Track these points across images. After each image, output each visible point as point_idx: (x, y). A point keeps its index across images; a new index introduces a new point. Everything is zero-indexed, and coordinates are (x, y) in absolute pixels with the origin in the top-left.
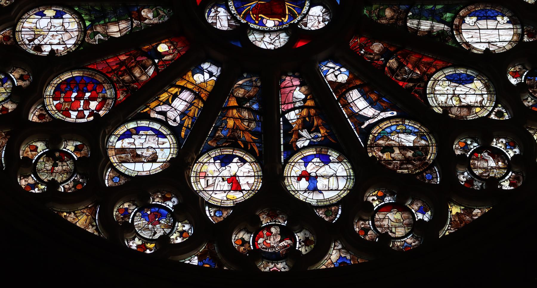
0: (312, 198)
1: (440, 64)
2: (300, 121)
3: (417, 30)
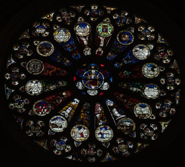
0: (102, 140)
1: (138, 101)
2: (100, 117)
3: (133, 91)
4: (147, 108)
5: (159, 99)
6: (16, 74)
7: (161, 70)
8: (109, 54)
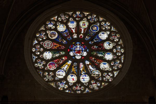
0: (84, 82)
1: (102, 61)
4: (107, 65)
5: (114, 60)
6: (38, 49)
7: (114, 45)
8: (87, 37)
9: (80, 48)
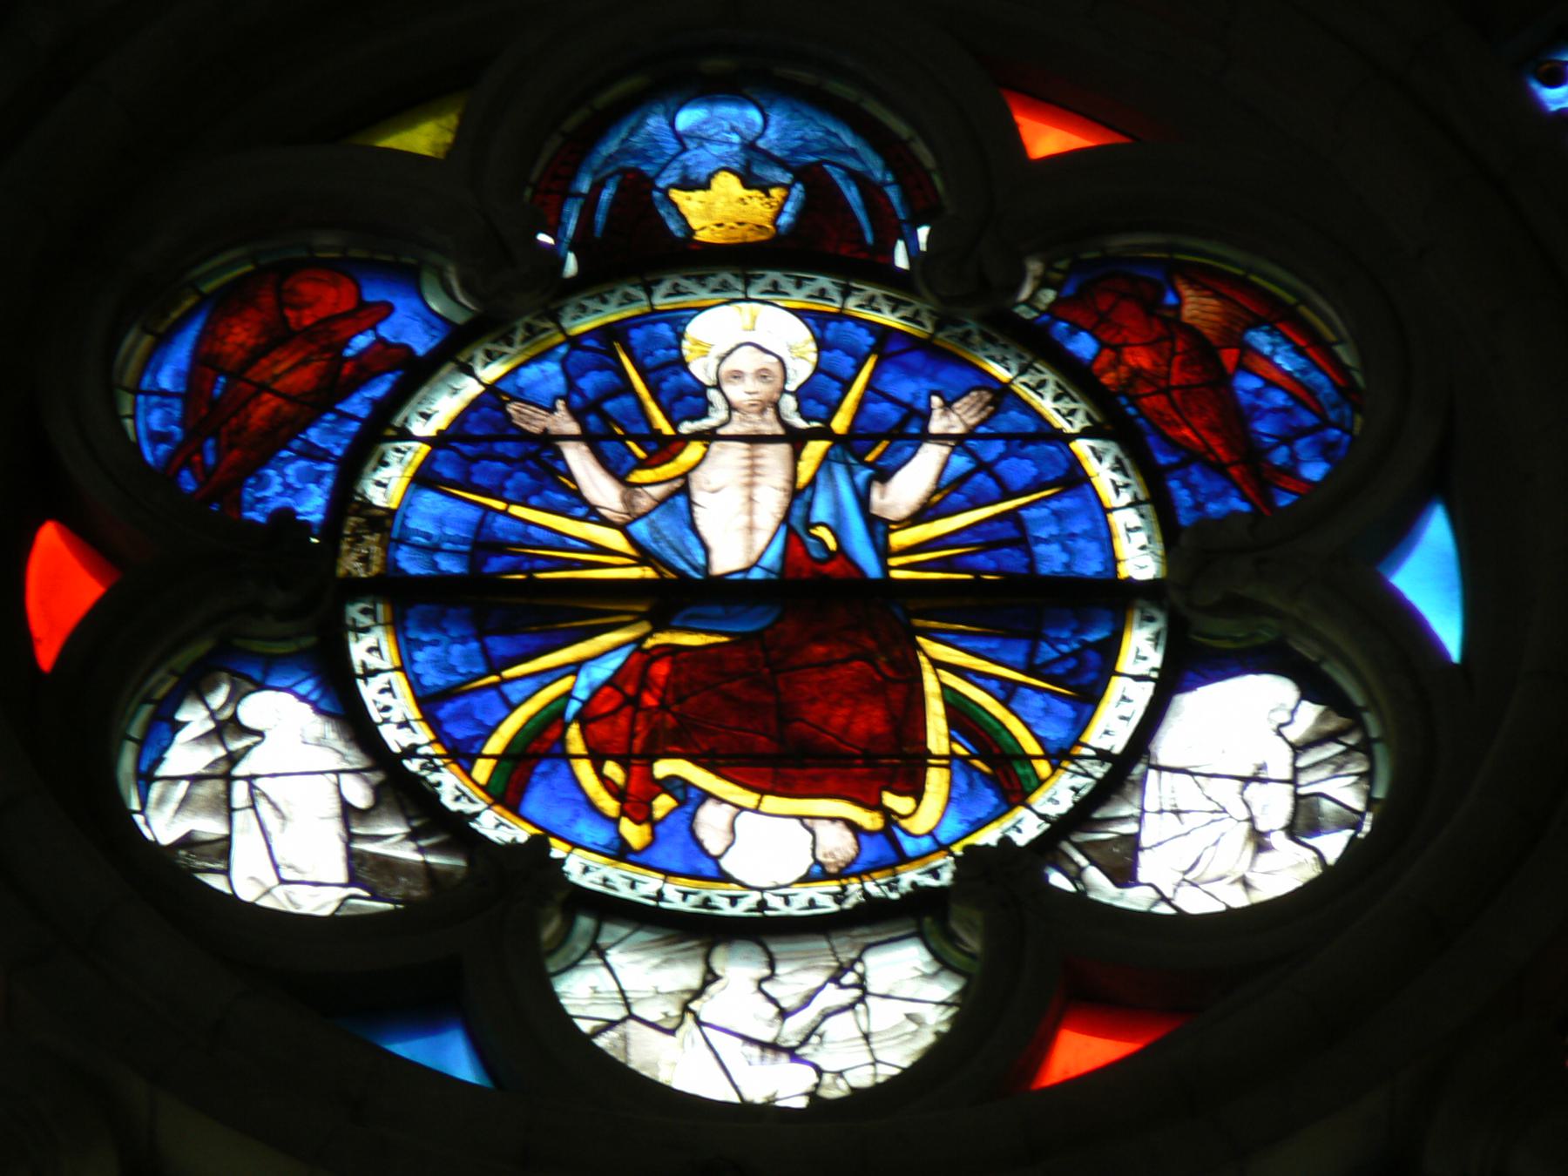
9: (876, 445)
